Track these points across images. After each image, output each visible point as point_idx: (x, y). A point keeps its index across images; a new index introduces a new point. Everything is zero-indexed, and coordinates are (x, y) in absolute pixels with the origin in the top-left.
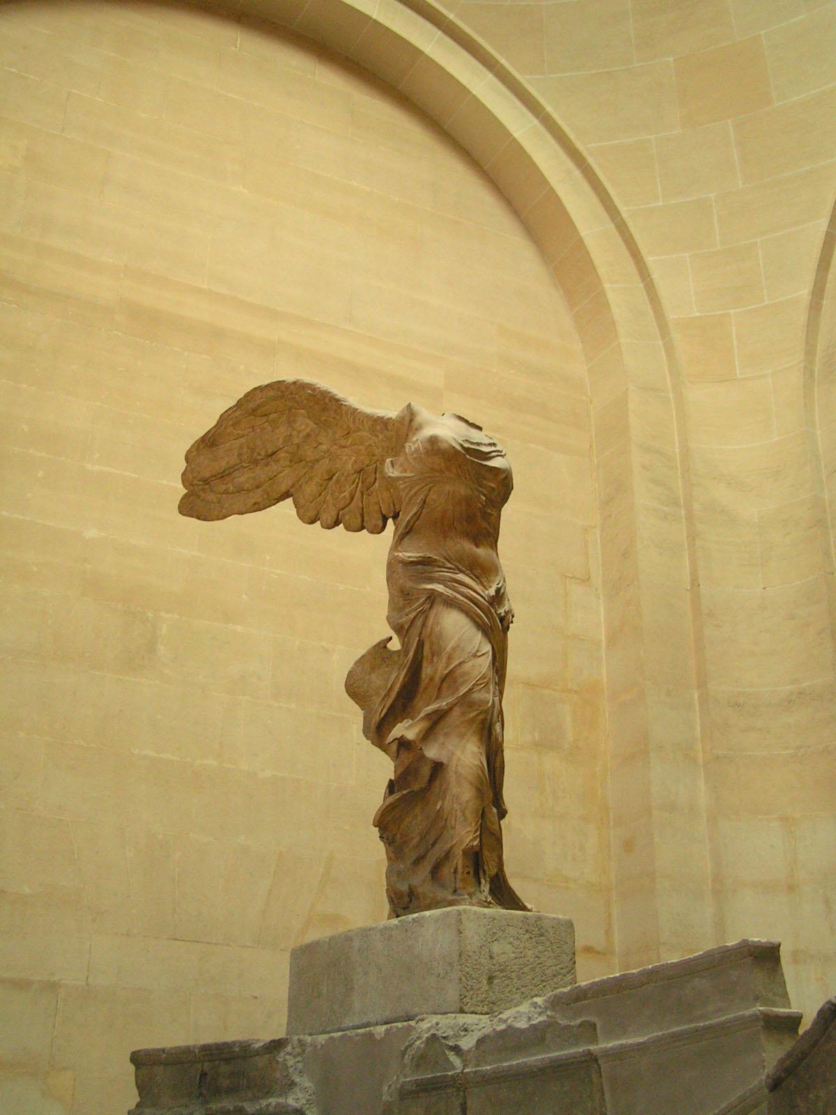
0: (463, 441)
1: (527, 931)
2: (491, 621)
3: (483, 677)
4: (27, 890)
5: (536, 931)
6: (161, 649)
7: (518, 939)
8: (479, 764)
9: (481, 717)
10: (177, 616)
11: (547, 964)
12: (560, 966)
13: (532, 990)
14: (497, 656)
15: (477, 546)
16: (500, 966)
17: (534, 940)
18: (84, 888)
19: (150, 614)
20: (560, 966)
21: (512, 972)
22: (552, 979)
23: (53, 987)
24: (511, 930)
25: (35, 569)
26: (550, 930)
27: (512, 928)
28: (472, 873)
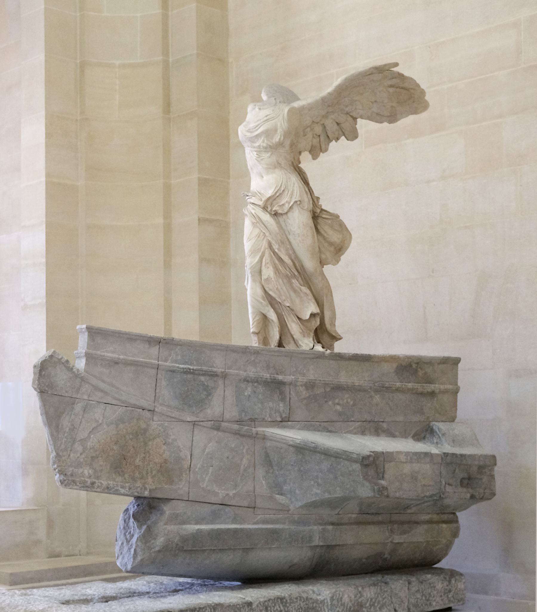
14: (267, 234)
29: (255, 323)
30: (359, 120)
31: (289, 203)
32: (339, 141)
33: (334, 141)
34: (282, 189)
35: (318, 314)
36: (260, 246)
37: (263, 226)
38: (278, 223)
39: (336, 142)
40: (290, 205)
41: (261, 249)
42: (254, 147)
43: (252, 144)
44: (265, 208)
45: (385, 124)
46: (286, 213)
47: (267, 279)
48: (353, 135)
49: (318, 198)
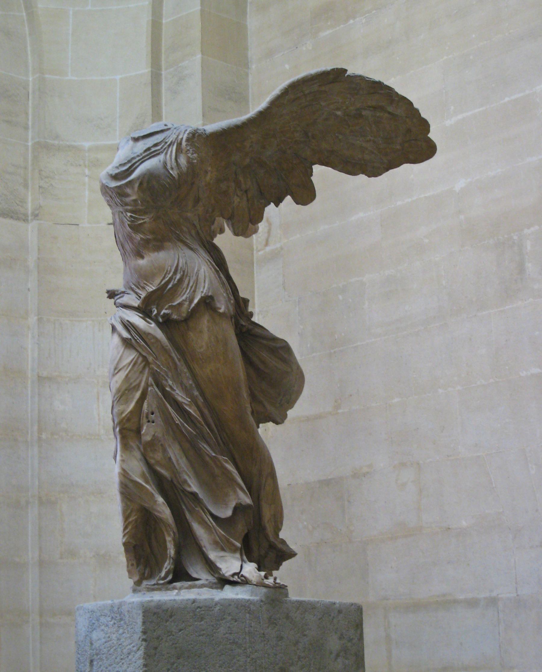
0: (117, 168)
1: (112, 618)
2: (132, 332)
3: (118, 390)
4: (464, 524)
5: (119, 618)
6: (529, 265)
7: (107, 626)
8: (122, 472)
9: (118, 429)
10: (537, 227)
11: (124, 644)
12: (133, 645)
13: (115, 667)
14: (150, 359)
15: (142, 257)
16: (97, 650)
17: (116, 625)
18: (503, 512)
19: (515, 238)
20: (133, 645)
21: (103, 654)
22: (128, 657)
23: (493, 601)
24: (103, 619)
25: (427, 241)
26: (126, 614)
27: (103, 617)
28: (135, 564)
29: (130, 527)
30: (317, 169)
31: (191, 301)
32: (282, 205)
33: (272, 204)
34: (178, 277)
35: (248, 506)
36: (138, 381)
37: (143, 343)
38: (170, 339)
39: (277, 205)
40: (193, 305)
41: (139, 385)
42: (126, 204)
43: (124, 199)
44: (144, 310)
45: (362, 178)
46: (186, 320)
47: (152, 439)
48: (305, 194)
49: (246, 302)
